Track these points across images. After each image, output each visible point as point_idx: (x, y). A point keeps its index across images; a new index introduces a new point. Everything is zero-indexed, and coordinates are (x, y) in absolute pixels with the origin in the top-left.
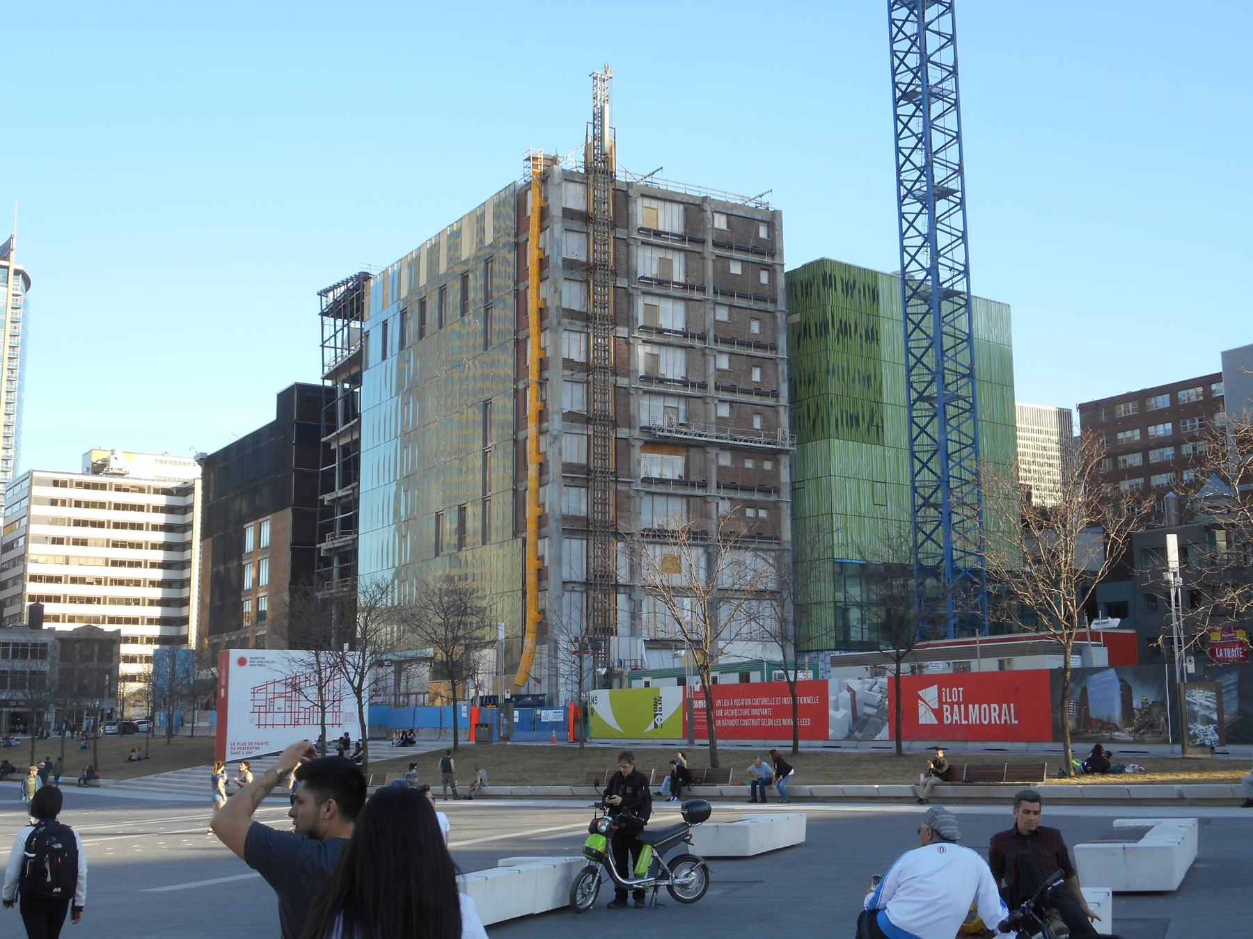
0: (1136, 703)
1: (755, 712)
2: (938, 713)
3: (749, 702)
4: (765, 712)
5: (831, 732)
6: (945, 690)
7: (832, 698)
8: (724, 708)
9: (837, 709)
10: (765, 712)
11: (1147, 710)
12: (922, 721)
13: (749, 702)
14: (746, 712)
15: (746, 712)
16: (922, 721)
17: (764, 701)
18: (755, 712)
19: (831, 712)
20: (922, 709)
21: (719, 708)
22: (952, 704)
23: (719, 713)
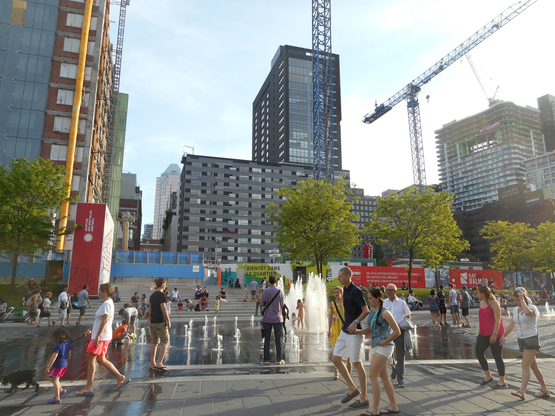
0: (525, 281)
1: (388, 277)
2: (468, 281)
3: (386, 274)
4: (395, 278)
5: (426, 285)
6: (470, 275)
7: (426, 274)
8: (371, 275)
9: (429, 278)
10: (395, 278)
11: (527, 282)
12: (462, 283)
13: (386, 274)
14: (384, 277)
15: (384, 277)
16: (462, 283)
17: (394, 274)
18: (388, 277)
19: (426, 279)
20: (462, 279)
21: (368, 275)
22: (472, 278)
23: (369, 277)
